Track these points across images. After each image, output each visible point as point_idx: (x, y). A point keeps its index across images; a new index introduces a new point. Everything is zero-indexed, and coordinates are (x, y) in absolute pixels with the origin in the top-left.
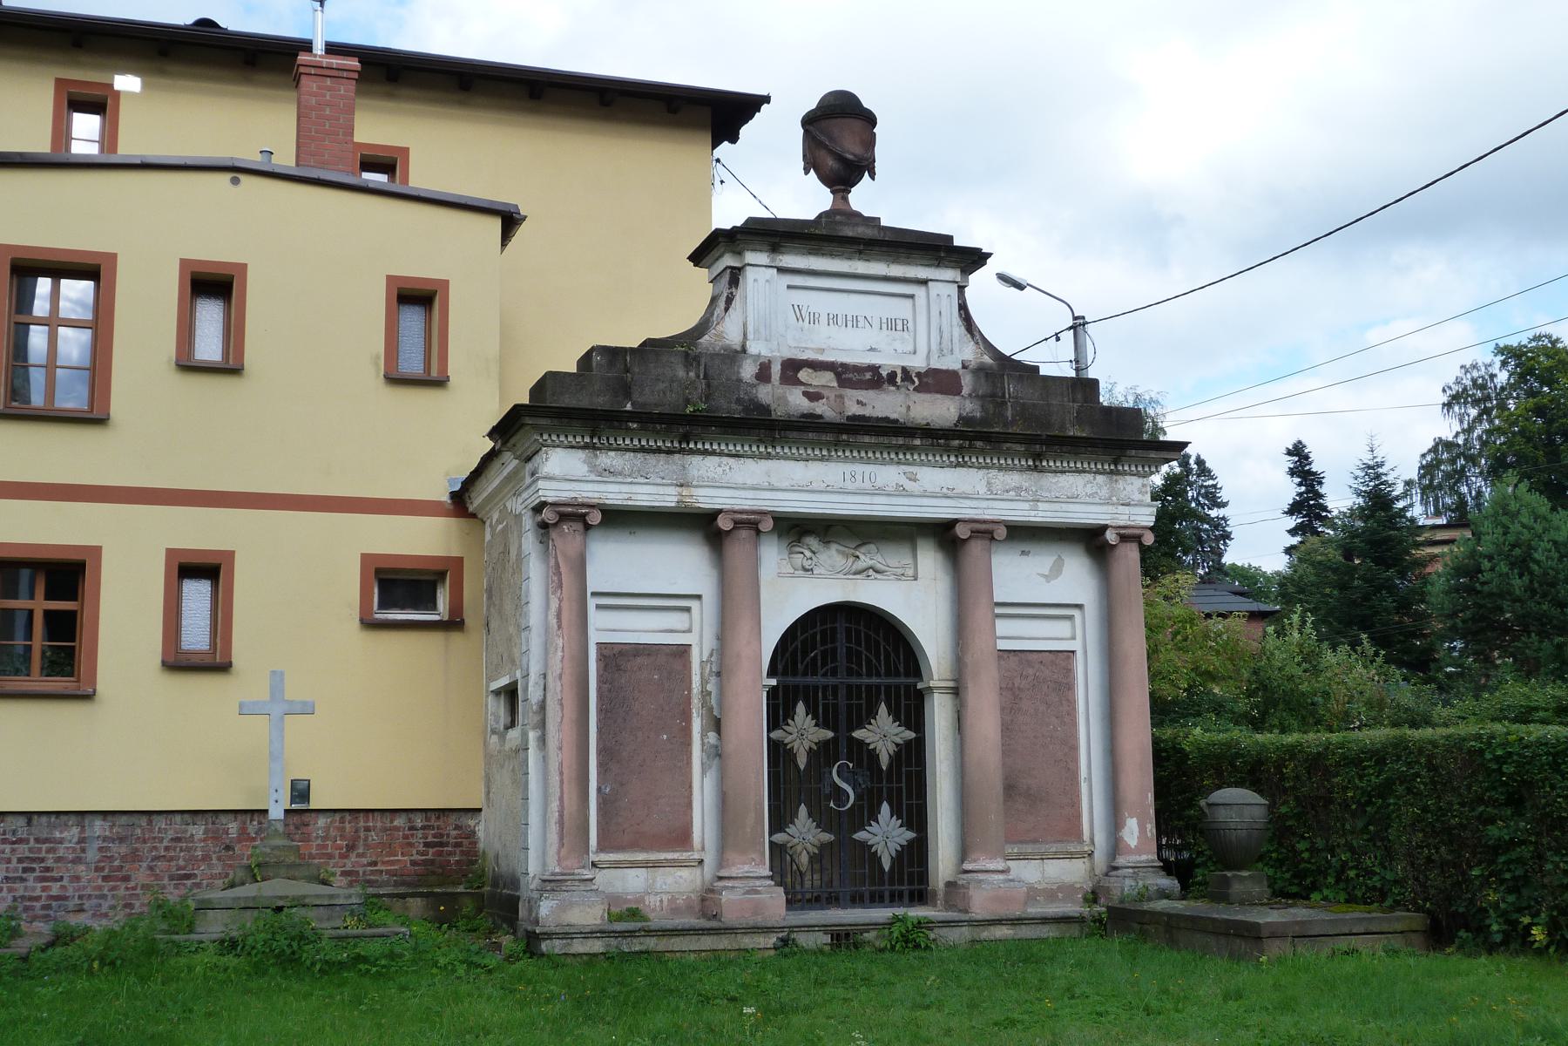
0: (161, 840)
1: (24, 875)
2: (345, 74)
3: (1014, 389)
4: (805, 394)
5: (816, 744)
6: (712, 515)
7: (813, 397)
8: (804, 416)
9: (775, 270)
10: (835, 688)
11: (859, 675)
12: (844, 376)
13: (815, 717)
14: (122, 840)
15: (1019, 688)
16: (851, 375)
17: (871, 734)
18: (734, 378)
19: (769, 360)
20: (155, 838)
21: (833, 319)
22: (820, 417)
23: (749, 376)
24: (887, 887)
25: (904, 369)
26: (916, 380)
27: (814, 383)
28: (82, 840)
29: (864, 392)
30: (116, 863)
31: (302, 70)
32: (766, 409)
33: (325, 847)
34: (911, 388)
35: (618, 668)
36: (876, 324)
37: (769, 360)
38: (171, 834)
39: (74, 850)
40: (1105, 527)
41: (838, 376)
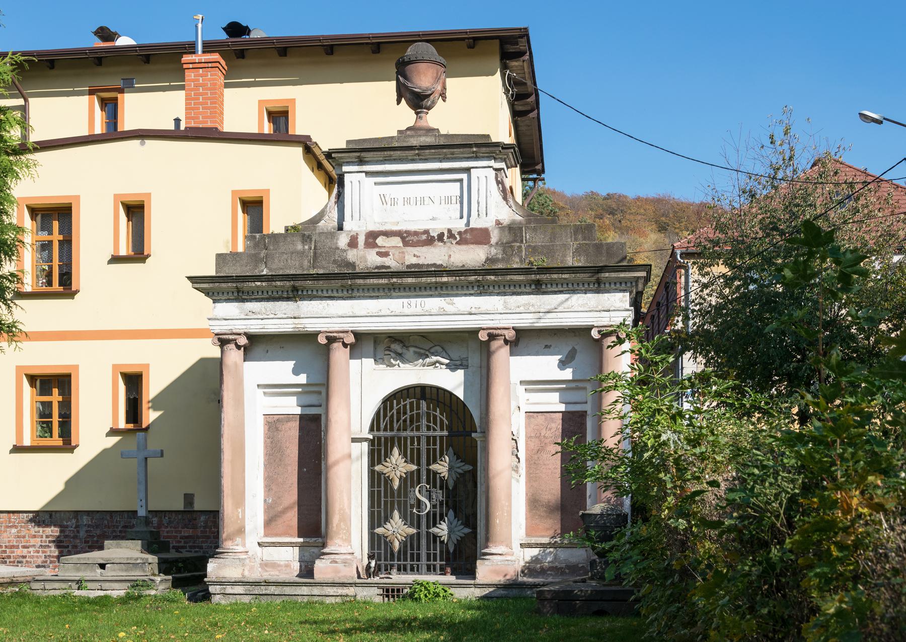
0: (117, 528)
2: (210, 65)
4: (379, 254)
5: (405, 473)
6: (314, 335)
8: (377, 267)
9: (364, 174)
10: (419, 438)
11: (435, 430)
13: (405, 456)
14: (97, 526)
15: (544, 437)
17: (441, 467)
21: (407, 201)
22: (389, 267)
24: (396, 562)
25: (449, 231)
26: (458, 237)
28: (77, 527)
29: (418, 248)
30: (95, 539)
31: (185, 66)
32: (353, 265)
34: (454, 242)
35: (277, 429)
36: (437, 201)
38: (122, 524)
41: (403, 239)
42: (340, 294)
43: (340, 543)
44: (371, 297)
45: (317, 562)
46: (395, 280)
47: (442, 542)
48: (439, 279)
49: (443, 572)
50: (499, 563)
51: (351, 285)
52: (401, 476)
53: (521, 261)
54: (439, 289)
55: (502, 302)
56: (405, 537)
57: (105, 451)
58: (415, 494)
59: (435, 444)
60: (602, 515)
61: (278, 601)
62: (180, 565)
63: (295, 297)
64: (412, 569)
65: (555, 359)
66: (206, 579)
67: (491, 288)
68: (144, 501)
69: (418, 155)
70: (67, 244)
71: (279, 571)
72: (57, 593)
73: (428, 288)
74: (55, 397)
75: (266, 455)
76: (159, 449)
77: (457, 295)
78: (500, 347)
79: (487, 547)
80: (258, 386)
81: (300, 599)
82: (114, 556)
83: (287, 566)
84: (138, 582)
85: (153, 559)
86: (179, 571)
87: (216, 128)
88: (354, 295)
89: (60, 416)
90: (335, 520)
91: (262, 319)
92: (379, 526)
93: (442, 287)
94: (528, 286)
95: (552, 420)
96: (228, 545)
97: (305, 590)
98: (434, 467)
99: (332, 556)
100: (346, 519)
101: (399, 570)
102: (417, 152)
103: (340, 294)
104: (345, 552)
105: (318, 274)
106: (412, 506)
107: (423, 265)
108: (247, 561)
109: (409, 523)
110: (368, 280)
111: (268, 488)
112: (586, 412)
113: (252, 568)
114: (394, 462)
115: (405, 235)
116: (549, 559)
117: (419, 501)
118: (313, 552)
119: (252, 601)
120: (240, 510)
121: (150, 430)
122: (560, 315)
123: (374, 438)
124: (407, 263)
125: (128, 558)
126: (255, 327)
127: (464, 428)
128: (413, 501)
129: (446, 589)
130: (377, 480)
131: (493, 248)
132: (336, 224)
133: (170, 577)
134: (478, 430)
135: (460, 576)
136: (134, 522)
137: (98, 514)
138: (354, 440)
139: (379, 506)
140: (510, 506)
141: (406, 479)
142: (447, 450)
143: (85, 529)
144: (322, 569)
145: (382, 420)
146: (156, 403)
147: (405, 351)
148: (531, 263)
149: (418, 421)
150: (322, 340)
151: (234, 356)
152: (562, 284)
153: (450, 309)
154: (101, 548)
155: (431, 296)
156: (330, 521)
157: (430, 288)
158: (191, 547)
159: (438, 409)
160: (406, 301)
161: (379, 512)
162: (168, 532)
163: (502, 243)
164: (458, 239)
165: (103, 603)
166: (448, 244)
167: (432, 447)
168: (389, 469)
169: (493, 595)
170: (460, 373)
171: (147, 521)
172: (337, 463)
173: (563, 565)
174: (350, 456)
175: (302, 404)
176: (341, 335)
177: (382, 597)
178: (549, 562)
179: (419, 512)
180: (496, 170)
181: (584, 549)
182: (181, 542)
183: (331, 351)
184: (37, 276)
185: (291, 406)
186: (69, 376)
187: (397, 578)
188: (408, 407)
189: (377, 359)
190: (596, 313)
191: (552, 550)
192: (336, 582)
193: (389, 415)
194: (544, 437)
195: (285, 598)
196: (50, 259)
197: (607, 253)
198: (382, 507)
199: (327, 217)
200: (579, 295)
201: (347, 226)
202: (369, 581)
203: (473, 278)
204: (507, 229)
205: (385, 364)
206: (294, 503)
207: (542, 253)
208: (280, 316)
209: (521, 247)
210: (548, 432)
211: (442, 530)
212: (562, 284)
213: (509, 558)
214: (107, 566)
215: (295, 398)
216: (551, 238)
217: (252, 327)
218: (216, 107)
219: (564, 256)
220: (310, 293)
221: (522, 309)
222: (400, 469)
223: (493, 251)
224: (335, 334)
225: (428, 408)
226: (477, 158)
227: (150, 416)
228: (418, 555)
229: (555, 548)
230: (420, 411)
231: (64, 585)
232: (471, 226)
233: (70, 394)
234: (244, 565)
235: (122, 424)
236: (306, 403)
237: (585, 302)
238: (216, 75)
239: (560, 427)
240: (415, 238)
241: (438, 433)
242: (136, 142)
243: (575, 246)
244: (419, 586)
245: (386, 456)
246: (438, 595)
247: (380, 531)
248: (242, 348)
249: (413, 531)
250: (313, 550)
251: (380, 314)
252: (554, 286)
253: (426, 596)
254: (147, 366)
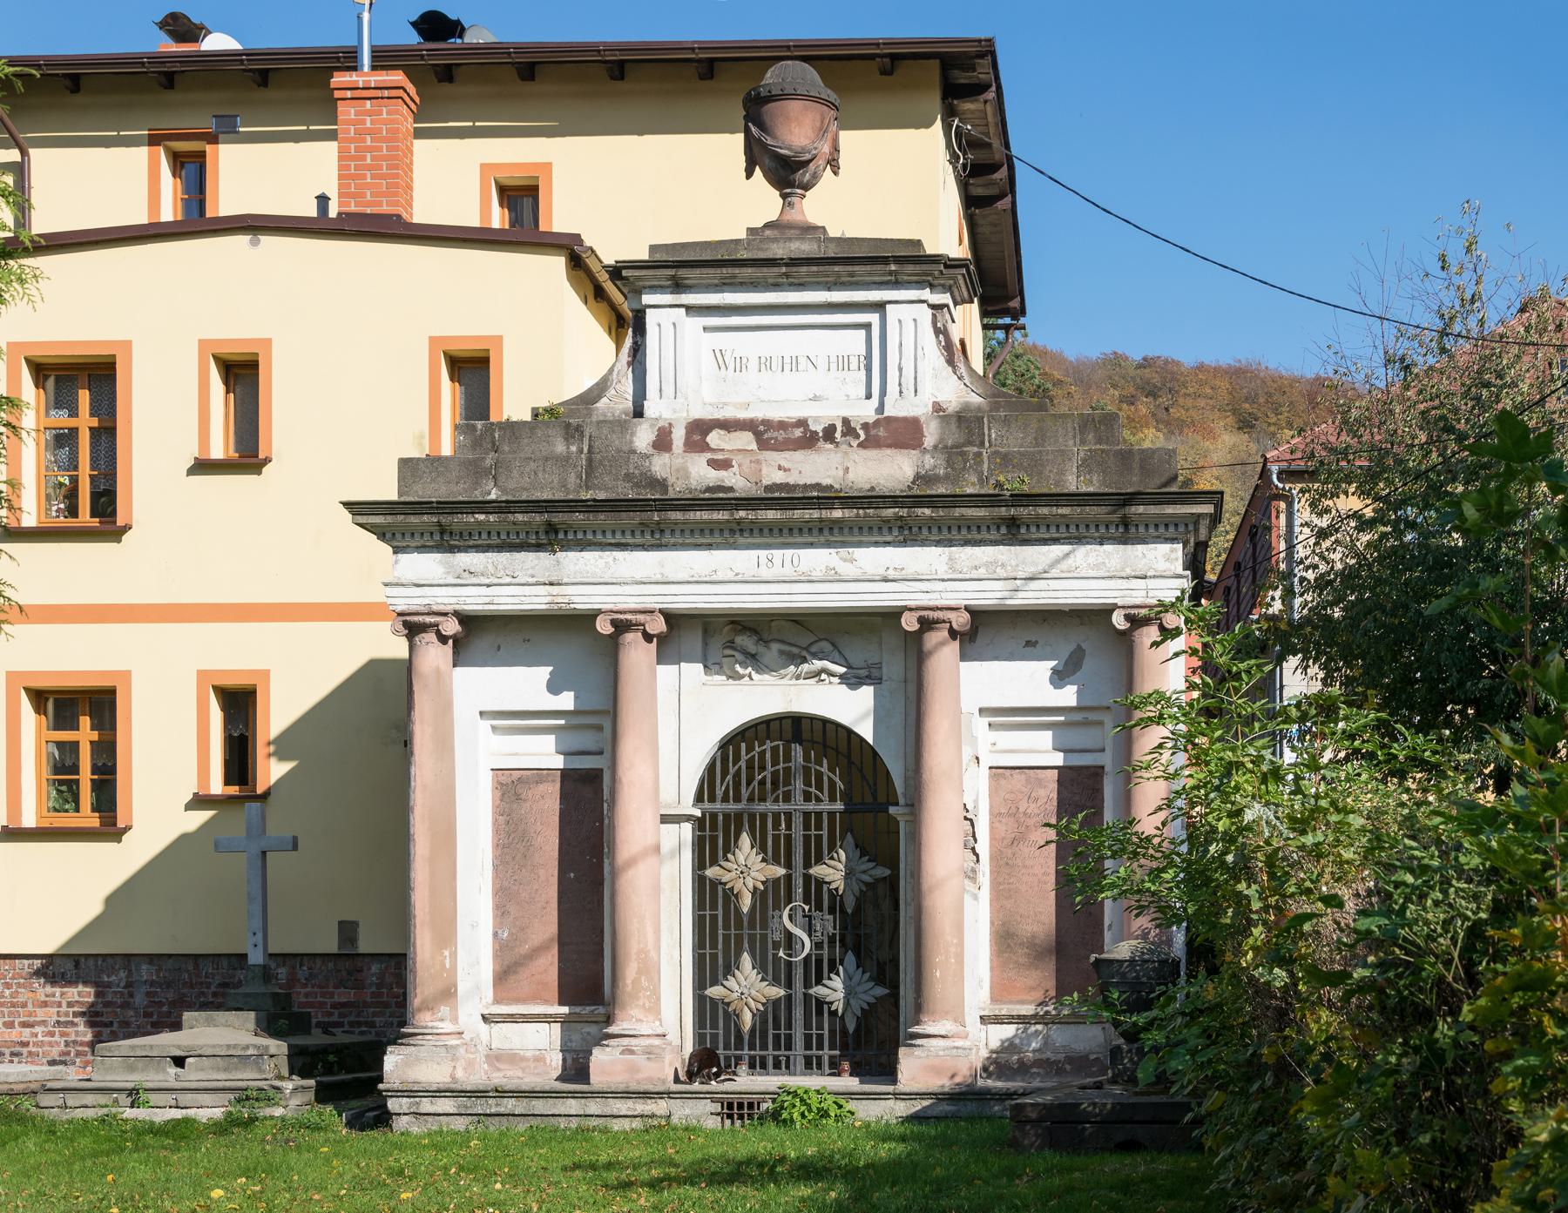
1: (76, 1020)
2: (386, 93)
3: (997, 435)
4: (714, 464)
8: (709, 489)
9: (683, 310)
10: (789, 815)
11: (818, 800)
12: (766, 436)
13: (763, 849)
14: (169, 985)
15: (1025, 814)
16: (775, 434)
17: (832, 871)
18: (625, 449)
19: (670, 424)
20: (201, 983)
21: (765, 364)
22: (731, 489)
24: (746, 1051)
25: (846, 422)
27: (727, 447)
28: (129, 985)
29: (787, 454)
30: (165, 1009)
31: (337, 94)
32: (662, 484)
33: (380, 995)
34: (855, 443)
35: (518, 798)
36: (822, 363)
37: (670, 424)
38: (218, 979)
39: (122, 994)
40: (1114, 607)
41: (758, 436)
42: (639, 540)
43: (641, 1016)
44: (697, 547)
45: (596, 1052)
46: (742, 514)
47: (833, 1014)
48: (825, 514)
49: (836, 1070)
50: (941, 1053)
51: (658, 523)
52: (755, 888)
53: (981, 481)
54: (826, 532)
55: (945, 558)
56: (763, 1004)
57: (184, 839)
58: (781, 922)
59: (819, 827)
60: (1132, 961)
61: (522, 1126)
62: (331, 1058)
63: (552, 545)
64: (777, 1065)
65: (1042, 669)
66: (381, 1086)
67: (925, 531)
68: (260, 935)
69: (787, 275)
70: (106, 435)
71: (523, 1070)
72: (90, 1113)
73: (805, 530)
74: (85, 733)
75: (496, 846)
76: (289, 834)
77: (859, 544)
78: (942, 644)
79: (918, 1023)
80: (481, 713)
81: (563, 1123)
82: (201, 1042)
83: (539, 1059)
84: (249, 1093)
85: (278, 1047)
86: (329, 1071)
87: (399, 216)
88: (664, 541)
89: (95, 770)
90: (630, 972)
91: (488, 586)
92: (714, 982)
93: (831, 529)
94: (993, 528)
95: (1041, 783)
96: (424, 1020)
97: (573, 1106)
98: (818, 871)
99: (625, 1041)
100: (651, 970)
101: (752, 1066)
102: (784, 269)
103: (639, 540)
104: (650, 1032)
105: (595, 500)
106: (776, 946)
107: (795, 487)
108: (462, 1050)
109: (770, 978)
110: (692, 513)
111: (501, 911)
112: (1103, 767)
113: (470, 1064)
114: (741, 860)
115: (762, 428)
116: (1034, 1045)
117: (789, 936)
118: (588, 1033)
119: (471, 1128)
120: (446, 953)
121: (271, 799)
122: (1054, 584)
123: (704, 814)
124: (766, 482)
125: (228, 1046)
126: (475, 600)
127: (875, 798)
128: (777, 936)
129: (842, 1102)
130: (709, 896)
131: (928, 457)
132: (630, 404)
133: (312, 1082)
134: (901, 801)
135: (867, 1078)
136: (240, 975)
137: (171, 961)
138: (666, 819)
139: (714, 945)
140: (961, 944)
141: (764, 894)
142: (842, 839)
143: (144, 989)
144: (605, 1063)
145: (718, 781)
146: (284, 746)
147: (761, 649)
148: (999, 485)
149: (787, 782)
150: (604, 627)
151: (434, 656)
152: (1058, 526)
153: (846, 570)
154: (176, 1026)
155: (811, 545)
156: (619, 973)
157: (810, 529)
158: (352, 1024)
159: (825, 761)
160: (763, 553)
161: (714, 957)
162: (307, 995)
163: (946, 447)
164: (863, 437)
165: (180, 1132)
166: (844, 447)
167: (813, 832)
168: (733, 874)
169: (929, 1113)
170: (867, 693)
171: (266, 973)
172: (632, 862)
173: (1061, 1057)
174: (657, 849)
175: (567, 749)
176: (641, 618)
177: (719, 1118)
178: (1034, 1051)
179: (790, 956)
180: (933, 307)
181: (1099, 1027)
182: (331, 1014)
183: (622, 648)
184: (48, 497)
185: (544, 753)
186: (111, 692)
187: (746, 1082)
188: (768, 755)
189: (709, 664)
190: (1120, 581)
191: (1039, 1027)
192: (631, 1089)
193: (732, 770)
194: (1025, 814)
195: (534, 1122)
196: (73, 464)
197: (1141, 467)
198: (720, 946)
199: (613, 392)
200: (1089, 547)
201: (652, 407)
202: (696, 1086)
203: (890, 512)
204: (954, 419)
205: (724, 674)
206: (552, 940)
207: (1019, 467)
208: (523, 581)
209: (981, 453)
210: (1033, 806)
211: (834, 990)
212: (1058, 526)
213: (959, 1043)
214: (189, 1060)
215: (552, 737)
216: (1036, 439)
217: (469, 600)
218: (397, 176)
219: (1062, 472)
220: (580, 536)
221: (982, 572)
222: (753, 874)
223: (929, 461)
224: (629, 617)
225: (807, 758)
226: (897, 284)
227: (272, 771)
228: (789, 1038)
229: (1046, 1024)
230: (792, 765)
231: (102, 1099)
232: (886, 414)
233: (113, 728)
234: (454, 1059)
235: (217, 787)
236: (576, 747)
237: (1100, 560)
238: (397, 112)
239: (1055, 795)
240: (781, 435)
241: (825, 806)
242: (241, 241)
243: (1082, 454)
244: (790, 1098)
245: (727, 849)
246: (824, 1114)
247: (714, 992)
248: (451, 642)
249: (778, 992)
250: (587, 1030)
251: (714, 578)
252: (1043, 529)
253: (803, 1116)
254: (266, 673)
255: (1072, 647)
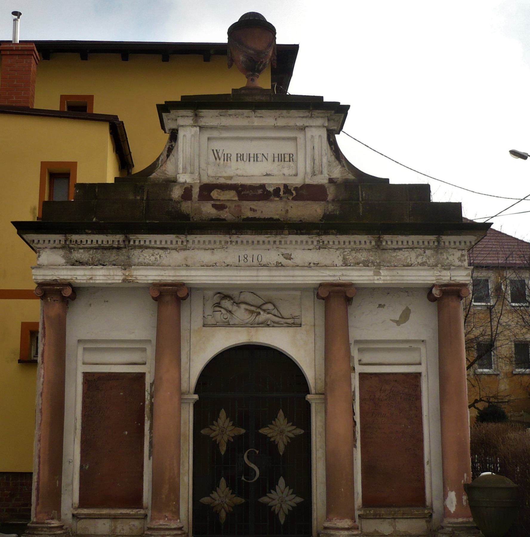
4: (214, 206)
7: (219, 207)
8: (212, 220)
12: (243, 193)
16: (248, 192)
21: (240, 157)
22: (224, 220)
23: (177, 197)
25: (286, 186)
26: (294, 192)
32: (186, 217)
34: (290, 198)
36: (270, 159)
41: (239, 193)
107: (259, 219)
131: (330, 205)
166: (285, 199)
223: (331, 207)
255: (404, 308)
